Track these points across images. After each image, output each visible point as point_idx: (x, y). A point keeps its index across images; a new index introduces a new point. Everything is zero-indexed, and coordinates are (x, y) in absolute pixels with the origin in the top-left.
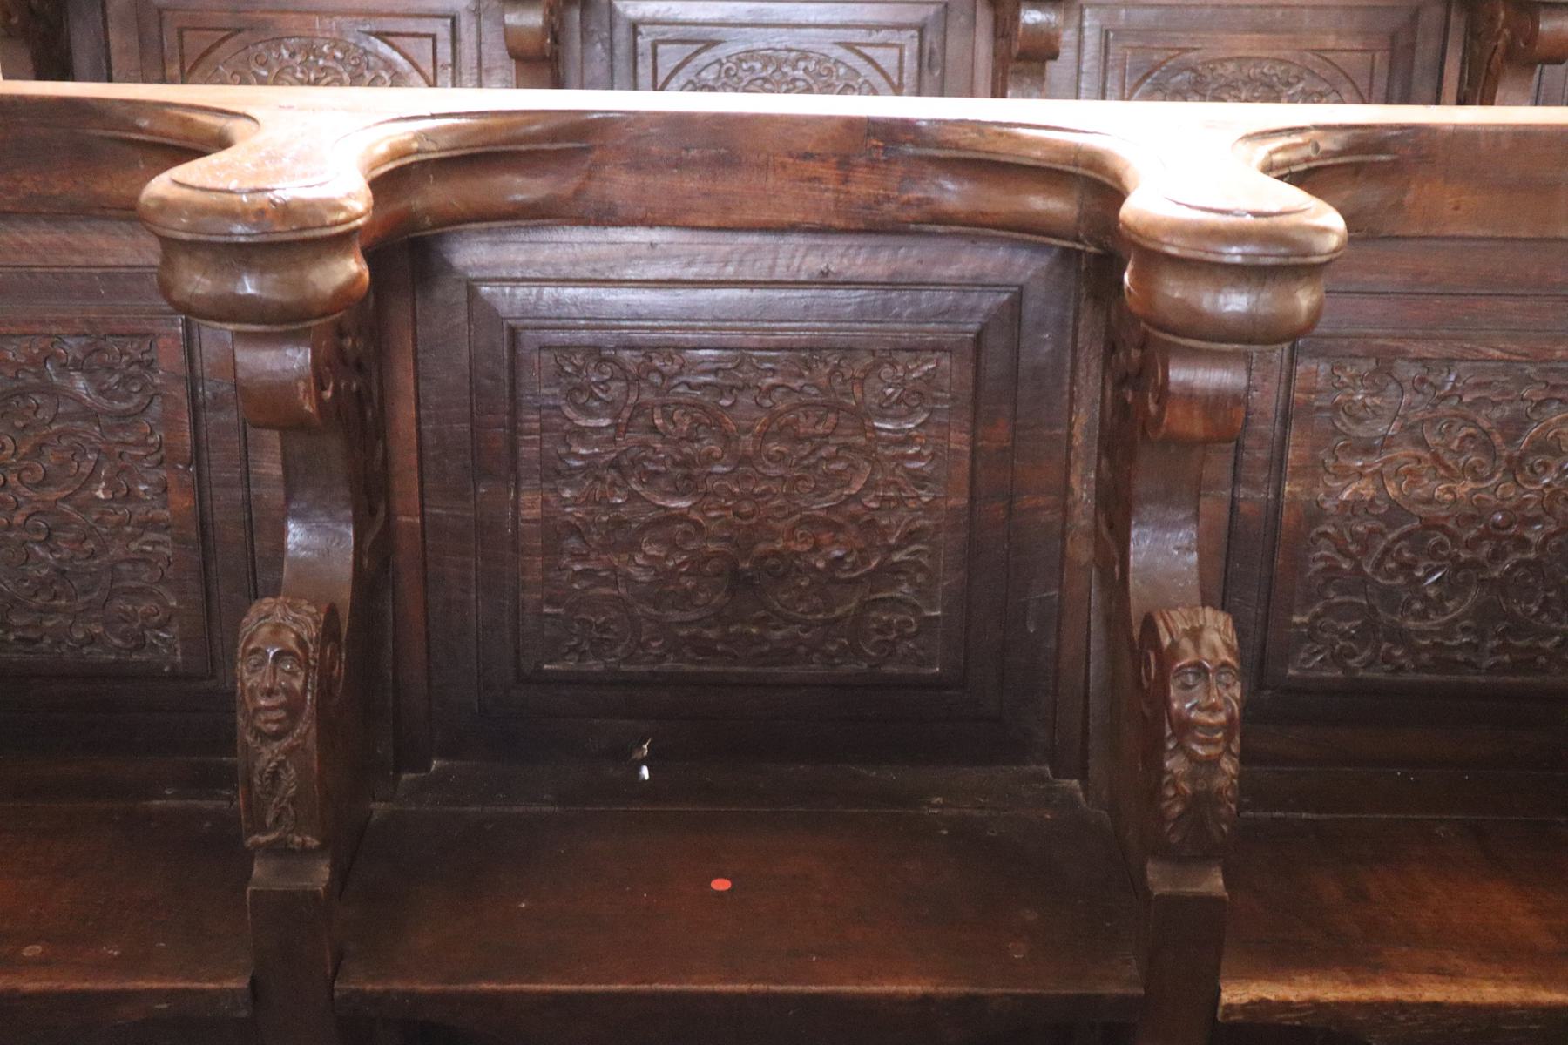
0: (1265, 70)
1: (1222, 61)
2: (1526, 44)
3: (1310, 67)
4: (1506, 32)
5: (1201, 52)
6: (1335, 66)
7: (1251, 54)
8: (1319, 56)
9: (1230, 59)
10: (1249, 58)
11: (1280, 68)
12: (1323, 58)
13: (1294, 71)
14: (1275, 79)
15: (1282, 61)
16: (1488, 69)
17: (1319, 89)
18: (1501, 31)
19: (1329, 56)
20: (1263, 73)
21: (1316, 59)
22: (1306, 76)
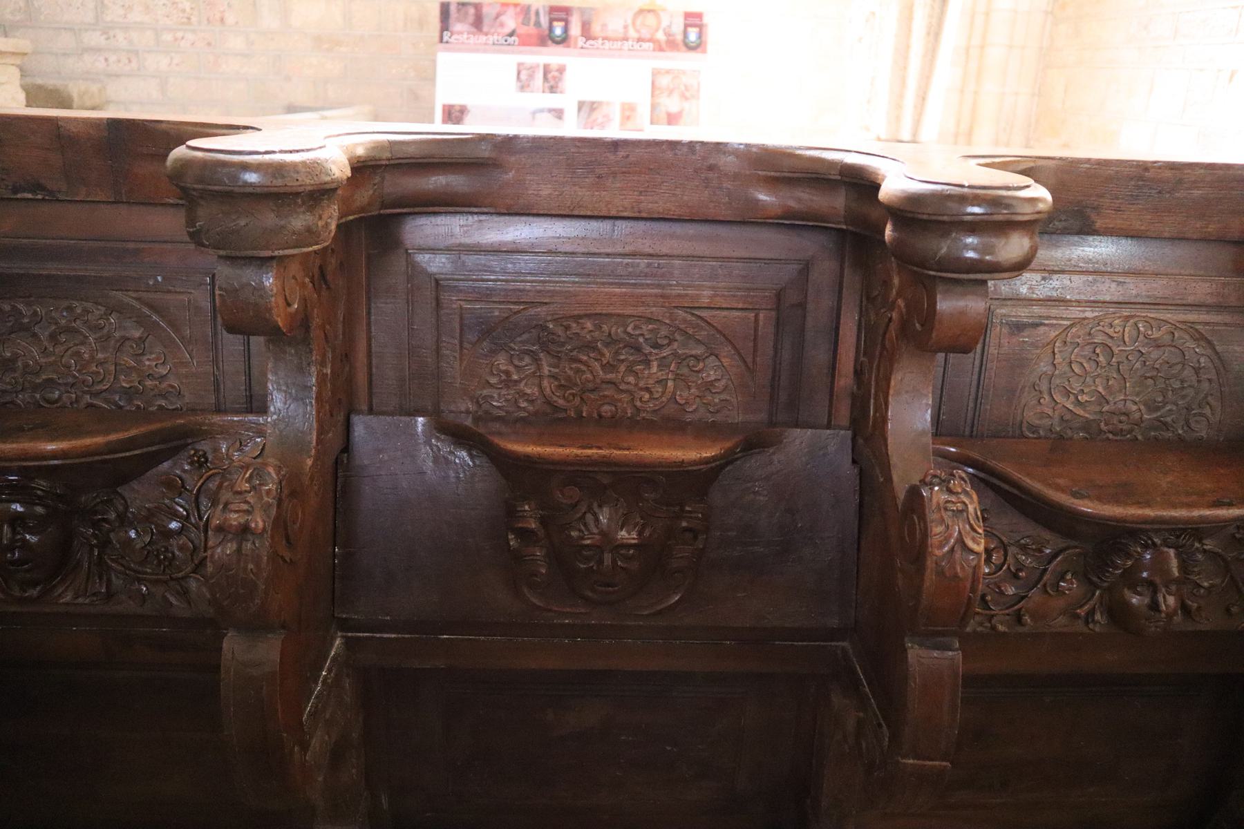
0: (629, 329)
1: (577, 318)
2: (922, 325)
3: (682, 326)
4: (900, 302)
5: (552, 307)
6: (713, 326)
7: (611, 310)
8: (693, 314)
9: (588, 316)
10: (610, 315)
11: (646, 328)
12: (693, 314)
13: (664, 332)
14: (641, 340)
15: (649, 320)
16: (883, 346)
17: (693, 352)
18: (894, 302)
19: (703, 314)
20: (625, 332)
21: (689, 317)
22: (677, 337)
